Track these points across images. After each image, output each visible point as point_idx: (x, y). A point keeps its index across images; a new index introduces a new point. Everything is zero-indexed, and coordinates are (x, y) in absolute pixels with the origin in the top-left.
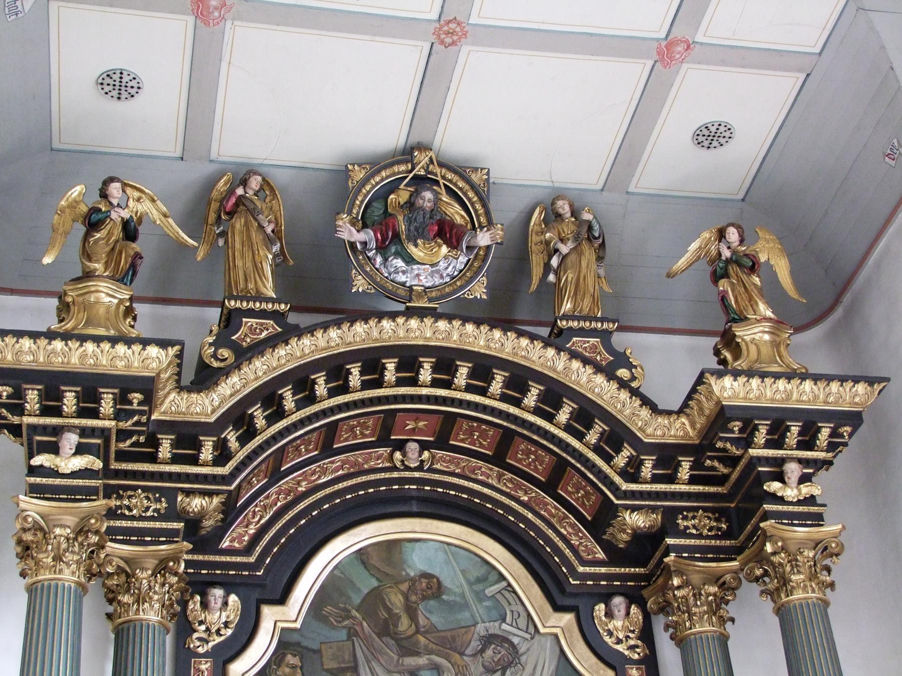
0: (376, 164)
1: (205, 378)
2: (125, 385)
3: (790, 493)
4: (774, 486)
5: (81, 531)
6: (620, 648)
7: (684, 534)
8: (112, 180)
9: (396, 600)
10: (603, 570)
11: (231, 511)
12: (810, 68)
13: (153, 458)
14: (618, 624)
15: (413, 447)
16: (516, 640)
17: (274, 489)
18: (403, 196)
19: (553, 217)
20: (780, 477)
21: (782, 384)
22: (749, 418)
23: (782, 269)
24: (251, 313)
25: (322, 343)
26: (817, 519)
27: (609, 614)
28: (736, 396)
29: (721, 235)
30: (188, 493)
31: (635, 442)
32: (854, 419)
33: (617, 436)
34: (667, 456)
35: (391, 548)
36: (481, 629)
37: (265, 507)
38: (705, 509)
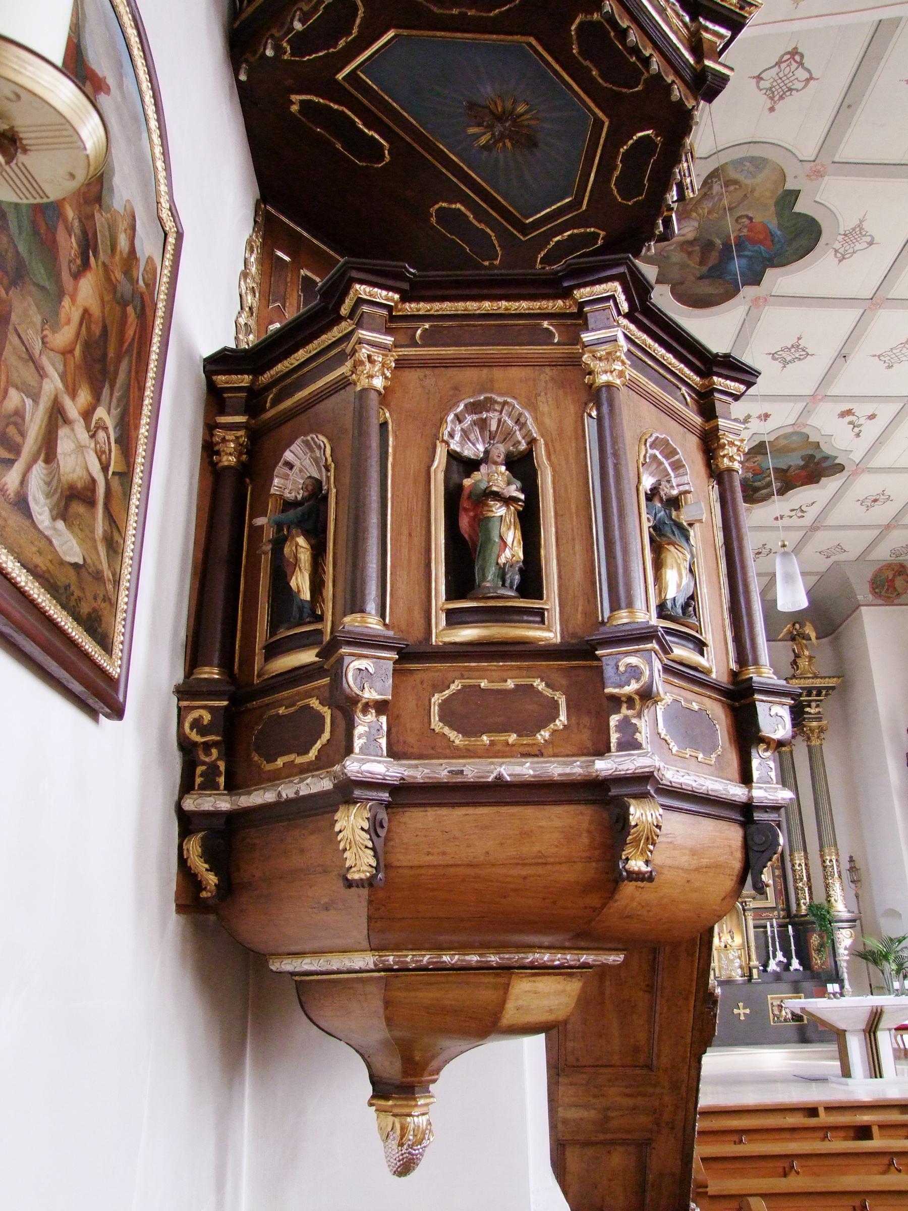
3: (812, 711)
4: (807, 709)
20: (809, 706)
21: (811, 680)
23: (813, 635)
29: (794, 625)
32: (833, 688)
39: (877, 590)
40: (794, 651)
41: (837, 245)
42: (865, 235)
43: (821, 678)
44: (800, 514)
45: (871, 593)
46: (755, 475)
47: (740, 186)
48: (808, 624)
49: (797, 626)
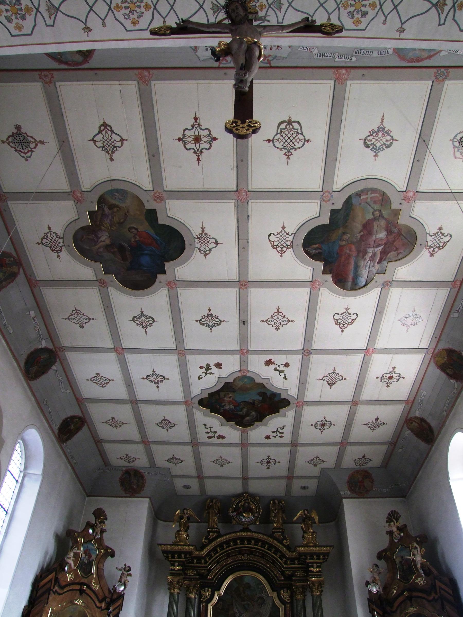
0: (237, 496)
1: (203, 547)
2: (186, 553)
3: (315, 570)
4: (311, 569)
5: (178, 582)
6: (286, 600)
7: (297, 576)
8: (185, 509)
9: (241, 589)
10: (283, 582)
11: (209, 571)
12: (319, 478)
13: (193, 563)
14: (285, 595)
15: (246, 555)
16: (264, 598)
17: (218, 566)
18: (243, 503)
19: (274, 503)
22: (306, 554)
23: (316, 518)
24: (212, 532)
25: (225, 538)
26: (320, 576)
27: (284, 592)
28: (302, 551)
30: (201, 570)
31: (286, 558)
32: (328, 554)
33: (283, 556)
34: (293, 561)
35: (241, 578)
36: (258, 595)
37: (216, 570)
38: (302, 570)
39: (353, 488)
40: (302, 527)
41: (198, 245)
42: (210, 238)
43: (319, 547)
44: (280, 435)
45: (349, 489)
46: (235, 407)
47: (120, 208)
48: (314, 511)
49: (306, 512)
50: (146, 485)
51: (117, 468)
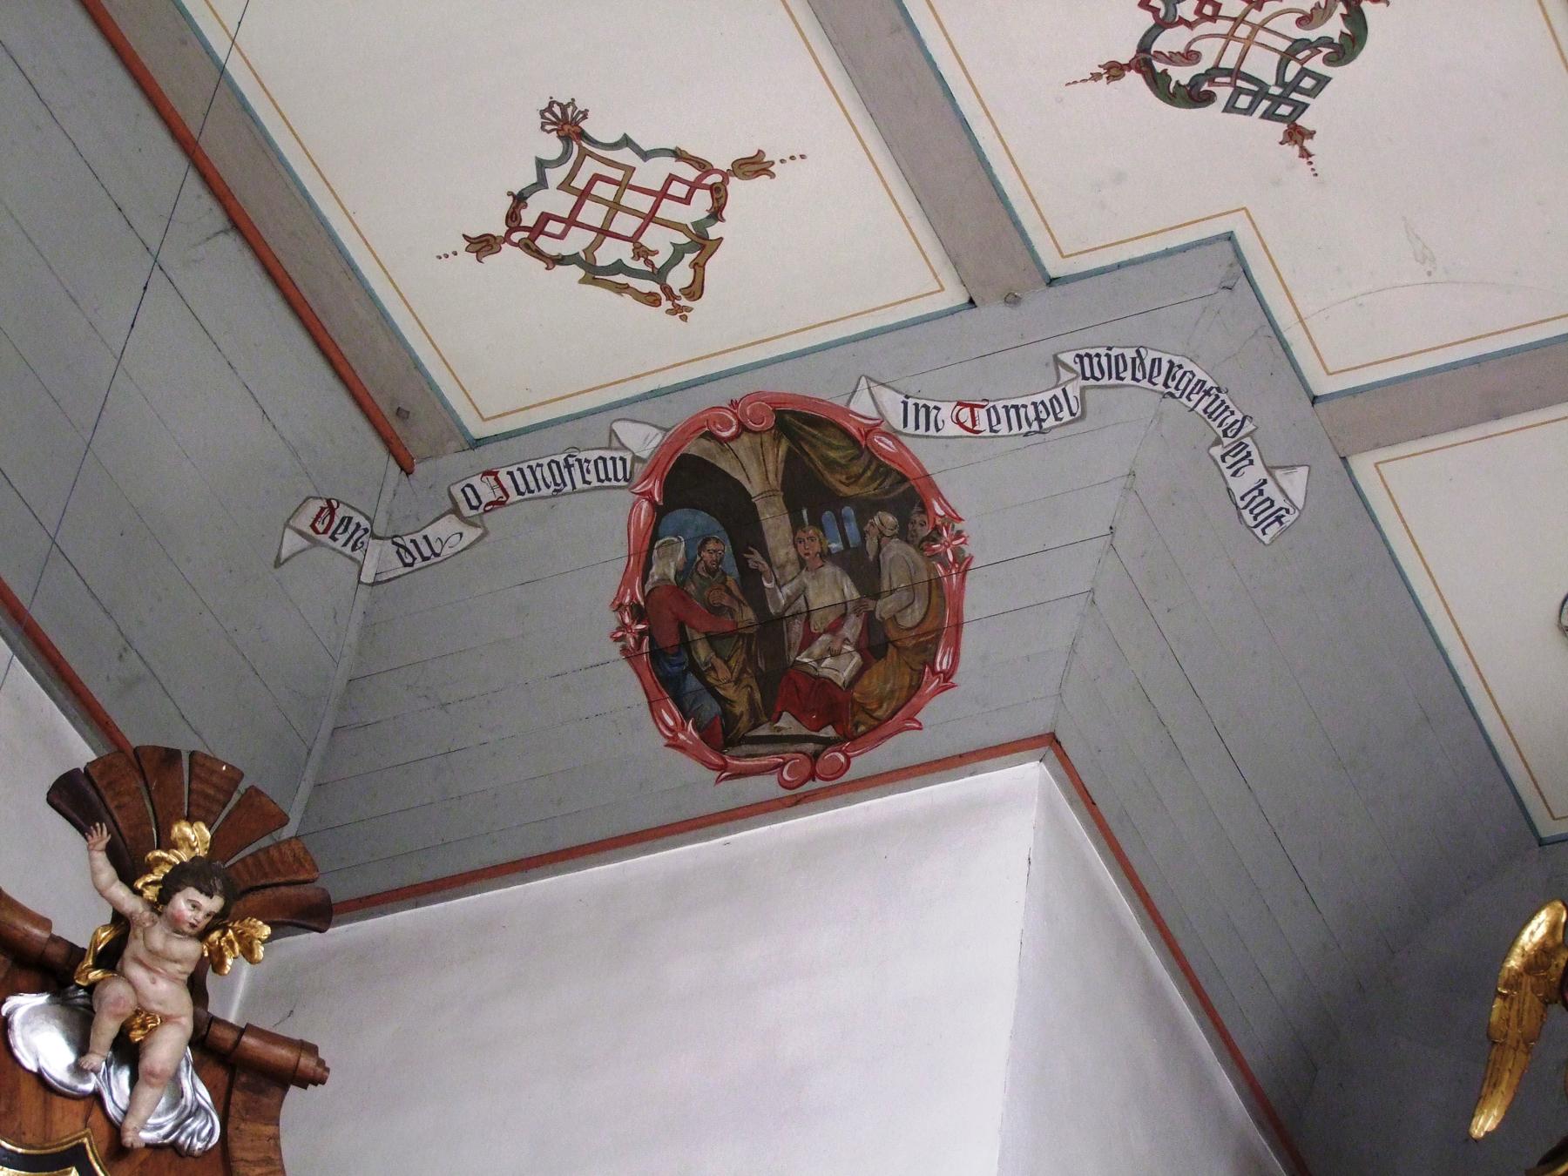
50: (978, 599)
51: (552, 456)
